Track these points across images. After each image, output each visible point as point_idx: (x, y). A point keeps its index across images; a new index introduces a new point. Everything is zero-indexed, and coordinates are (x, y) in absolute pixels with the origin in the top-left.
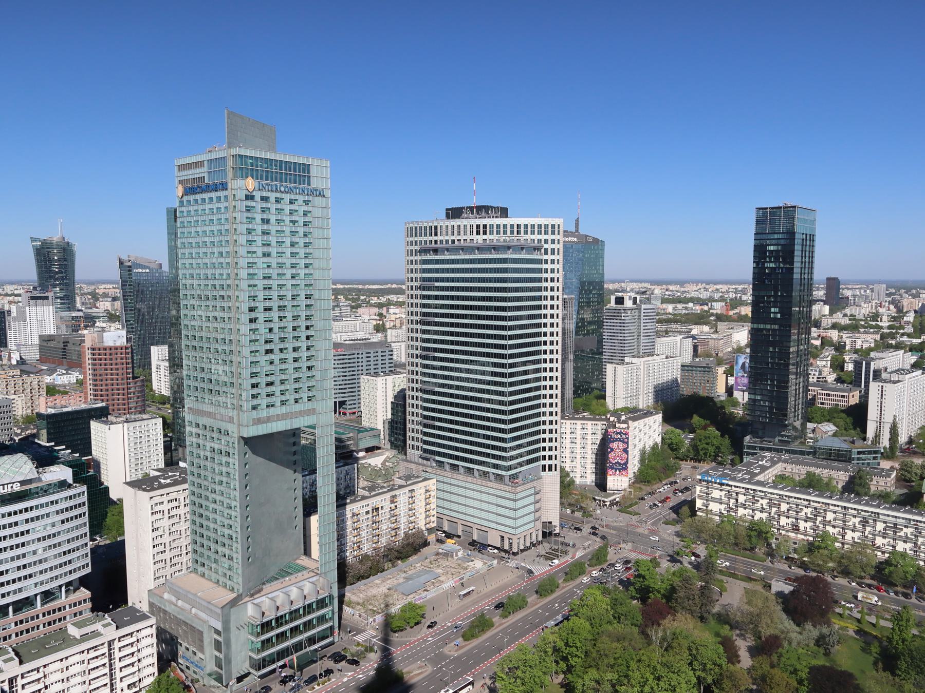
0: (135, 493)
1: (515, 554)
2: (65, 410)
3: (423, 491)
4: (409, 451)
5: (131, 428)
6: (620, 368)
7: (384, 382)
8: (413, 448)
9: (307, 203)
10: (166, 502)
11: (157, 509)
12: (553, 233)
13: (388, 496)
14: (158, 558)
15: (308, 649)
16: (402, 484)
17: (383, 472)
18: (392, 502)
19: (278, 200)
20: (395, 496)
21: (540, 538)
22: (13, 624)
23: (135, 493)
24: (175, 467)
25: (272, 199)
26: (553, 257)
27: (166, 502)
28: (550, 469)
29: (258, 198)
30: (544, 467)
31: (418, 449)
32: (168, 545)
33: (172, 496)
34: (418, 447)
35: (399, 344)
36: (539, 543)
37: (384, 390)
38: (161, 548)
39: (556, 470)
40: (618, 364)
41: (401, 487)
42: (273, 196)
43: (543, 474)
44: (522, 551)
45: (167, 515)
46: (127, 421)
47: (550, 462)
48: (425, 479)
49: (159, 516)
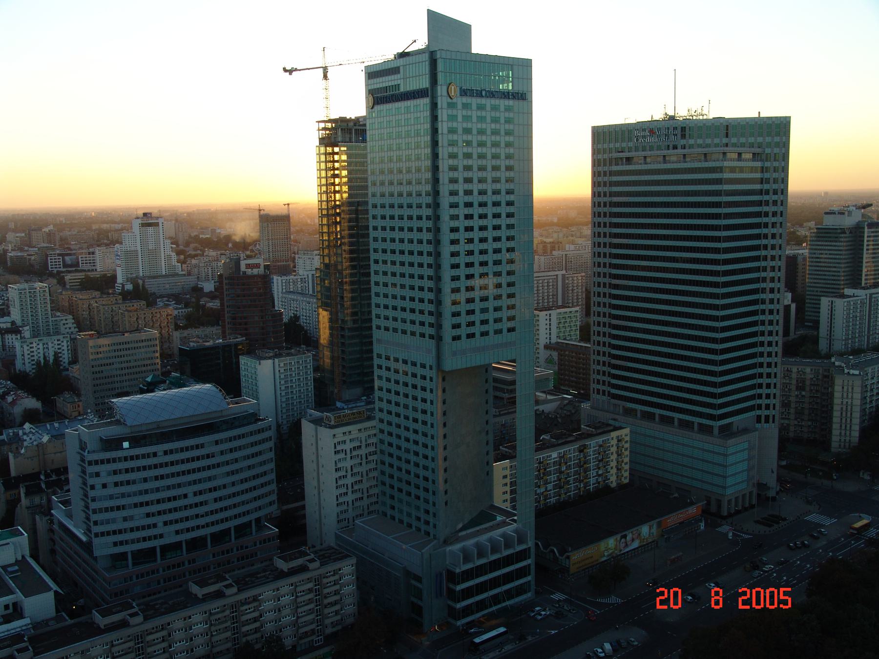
0: (316, 429)
1: (724, 518)
2: (207, 344)
3: (614, 442)
4: (594, 396)
5: (282, 365)
6: (839, 303)
7: (548, 317)
8: (598, 393)
9: (508, 109)
10: (348, 441)
11: (339, 448)
12: (778, 134)
13: (576, 446)
14: (341, 500)
15: (508, 603)
16: (589, 432)
17: (560, 420)
18: (581, 451)
19: (481, 107)
20: (585, 446)
21: (754, 501)
22: (211, 556)
23: (316, 429)
24: (333, 407)
25: (474, 107)
26: (776, 164)
27: (348, 441)
28: (767, 421)
29: (460, 106)
30: (759, 419)
31: (604, 394)
32: (350, 486)
33: (355, 434)
34: (604, 391)
35: (556, 273)
36: (752, 506)
37: (548, 327)
38: (344, 490)
39: (773, 422)
40: (835, 297)
41: (590, 436)
42: (474, 101)
43: (758, 426)
44: (738, 512)
45: (349, 456)
46: (276, 356)
47: (767, 412)
48: (616, 429)
49: (342, 456)
